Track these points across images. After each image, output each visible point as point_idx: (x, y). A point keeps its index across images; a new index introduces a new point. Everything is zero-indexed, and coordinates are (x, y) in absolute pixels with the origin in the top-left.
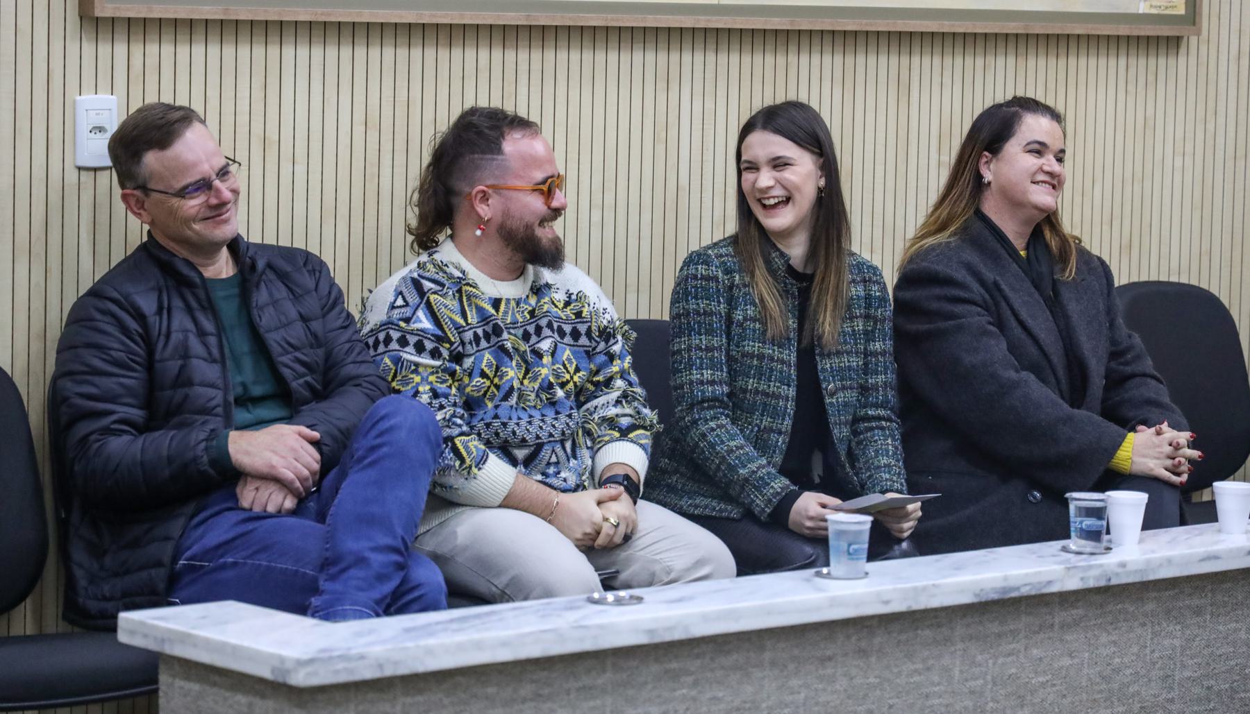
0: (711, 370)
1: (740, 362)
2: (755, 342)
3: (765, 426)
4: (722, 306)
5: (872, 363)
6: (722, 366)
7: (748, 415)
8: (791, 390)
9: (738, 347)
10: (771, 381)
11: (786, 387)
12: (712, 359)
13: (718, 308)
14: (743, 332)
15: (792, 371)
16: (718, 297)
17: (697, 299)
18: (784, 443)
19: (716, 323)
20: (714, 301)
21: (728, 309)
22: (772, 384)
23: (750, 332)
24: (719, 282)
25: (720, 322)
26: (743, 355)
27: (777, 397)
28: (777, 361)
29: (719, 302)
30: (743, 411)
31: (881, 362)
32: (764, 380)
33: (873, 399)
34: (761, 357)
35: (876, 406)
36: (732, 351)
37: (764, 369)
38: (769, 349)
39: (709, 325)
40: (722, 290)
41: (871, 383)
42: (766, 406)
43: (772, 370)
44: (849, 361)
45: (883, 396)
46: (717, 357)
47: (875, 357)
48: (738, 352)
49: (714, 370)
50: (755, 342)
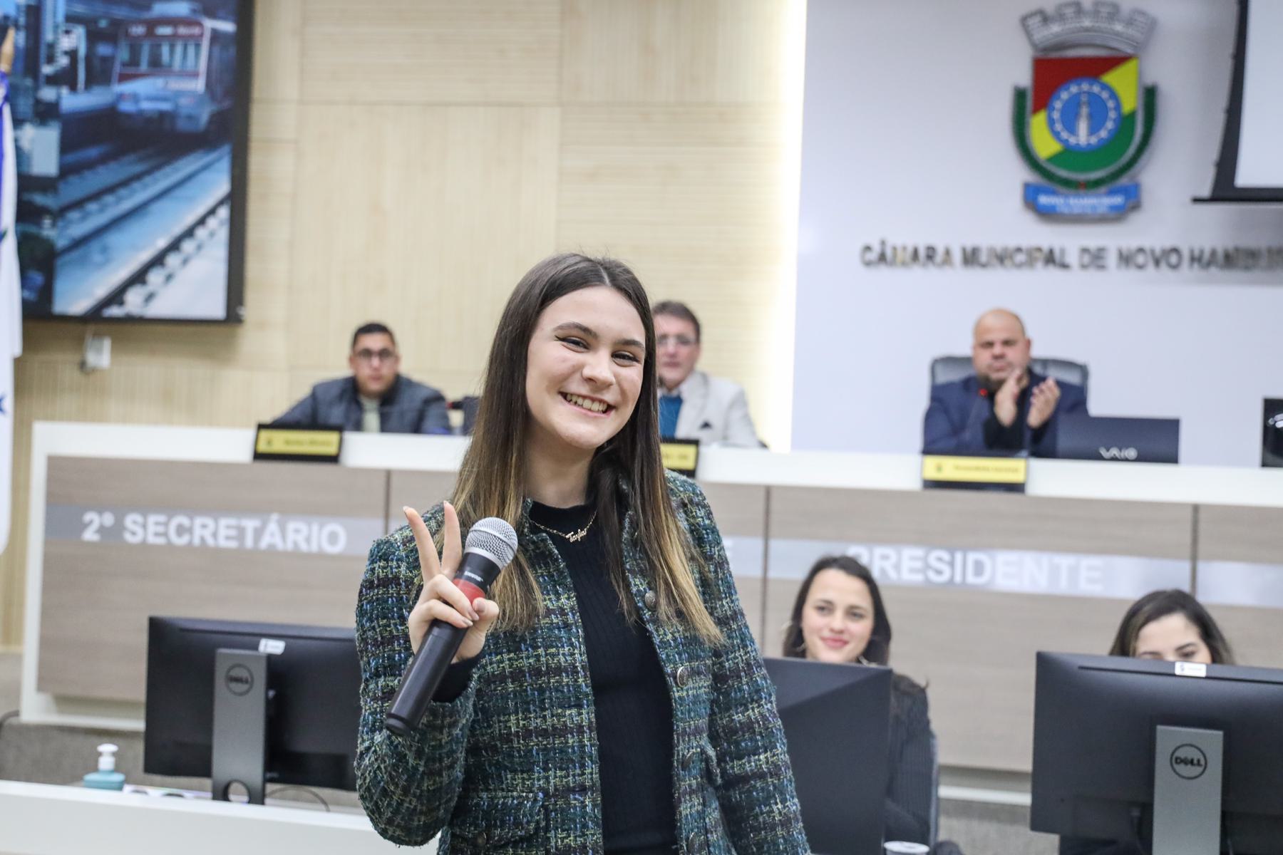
2: (501, 653)
3: (555, 786)
7: (525, 775)
8: (584, 711)
10: (544, 709)
11: (574, 711)
15: (580, 680)
18: (594, 806)
22: (547, 713)
27: (562, 731)
30: (514, 771)
32: (535, 711)
34: (517, 675)
37: (529, 692)
38: (528, 658)
42: (548, 754)
43: (541, 691)
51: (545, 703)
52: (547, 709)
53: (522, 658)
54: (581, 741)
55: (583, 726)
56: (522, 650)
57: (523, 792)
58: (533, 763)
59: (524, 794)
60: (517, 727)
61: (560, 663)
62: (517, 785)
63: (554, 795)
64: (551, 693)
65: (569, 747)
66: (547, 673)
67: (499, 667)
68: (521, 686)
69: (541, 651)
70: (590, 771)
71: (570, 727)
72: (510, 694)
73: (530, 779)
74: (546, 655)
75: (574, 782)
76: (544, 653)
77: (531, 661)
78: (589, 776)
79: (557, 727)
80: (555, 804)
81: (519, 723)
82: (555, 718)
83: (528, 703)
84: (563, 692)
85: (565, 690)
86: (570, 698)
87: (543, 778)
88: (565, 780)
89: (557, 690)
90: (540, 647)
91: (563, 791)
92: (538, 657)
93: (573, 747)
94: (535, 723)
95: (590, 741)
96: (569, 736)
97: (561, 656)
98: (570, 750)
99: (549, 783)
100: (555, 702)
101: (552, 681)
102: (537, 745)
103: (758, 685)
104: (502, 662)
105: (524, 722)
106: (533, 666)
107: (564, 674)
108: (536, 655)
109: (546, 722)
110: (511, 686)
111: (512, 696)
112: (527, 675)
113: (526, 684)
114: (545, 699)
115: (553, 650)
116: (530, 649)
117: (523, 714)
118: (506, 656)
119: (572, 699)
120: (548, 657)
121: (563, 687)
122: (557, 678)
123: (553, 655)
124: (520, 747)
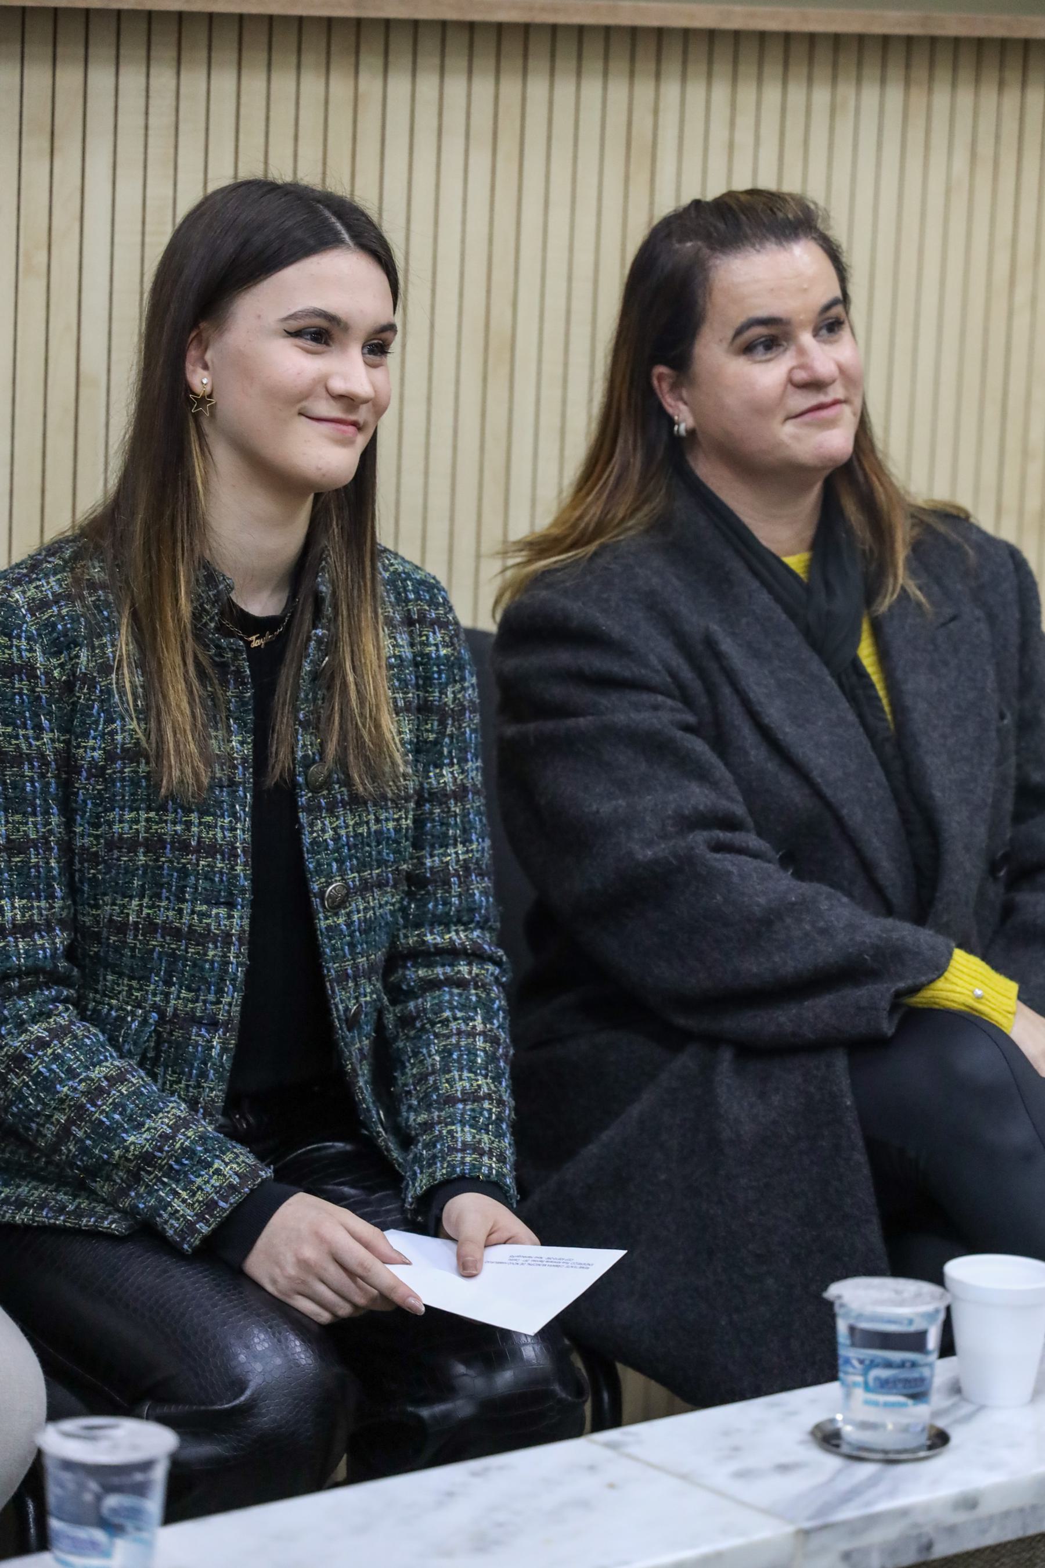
1: (105, 862)
2: (138, 809)
3: (176, 1009)
4: (46, 737)
7: (134, 983)
8: (236, 914)
10: (184, 901)
11: (223, 911)
15: (239, 868)
16: (36, 715)
19: (32, 781)
20: (24, 726)
21: (64, 741)
22: (187, 907)
24: (37, 677)
26: (110, 845)
27: (203, 938)
28: (197, 851)
30: (121, 975)
32: (168, 898)
34: (155, 845)
36: (82, 836)
38: (174, 823)
39: (14, 788)
40: (43, 696)
42: (174, 963)
43: (184, 873)
44: (378, 821)
48: (97, 837)
51: (185, 892)
52: (187, 901)
53: (166, 822)
54: (225, 956)
55: (233, 935)
56: (167, 811)
57: (127, 1003)
58: (151, 970)
59: (129, 1008)
60: (138, 917)
61: (216, 840)
62: (120, 992)
63: (170, 1022)
64: (197, 880)
65: (206, 961)
67: (131, 828)
68: (157, 860)
69: (194, 817)
70: (228, 1000)
71: (214, 933)
72: (137, 869)
73: (140, 989)
74: (200, 824)
75: (203, 1011)
77: (178, 828)
78: (227, 1008)
79: (196, 930)
80: (171, 1034)
81: (142, 911)
82: (195, 917)
83: (162, 886)
84: (212, 881)
85: (217, 879)
86: (220, 891)
87: (161, 994)
88: (190, 1005)
89: (206, 878)
90: (193, 812)
91: (184, 1019)
92: (188, 824)
93: (212, 962)
94: (165, 914)
95: (237, 957)
96: (210, 945)
97: (218, 830)
98: (207, 966)
99: (168, 1002)
100: (201, 894)
101: (202, 863)
102: (162, 946)
103: (474, 901)
104: (137, 821)
105: (149, 911)
106: (180, 836)
107: (219, 857)
108: (186, 821)
109: (181, 918)
110: (142, 858)
111: (140, 872)
112: (169, 846)
113: (163, 859)
114: (186, 886)
115: (209, 819)
116: (179, 810)
117: (150, 899)
118: (143, 815)
119: (223, 894)
121: (215, 873)
122: (210, 859)
123: (209, 827)
124: (135, 944)
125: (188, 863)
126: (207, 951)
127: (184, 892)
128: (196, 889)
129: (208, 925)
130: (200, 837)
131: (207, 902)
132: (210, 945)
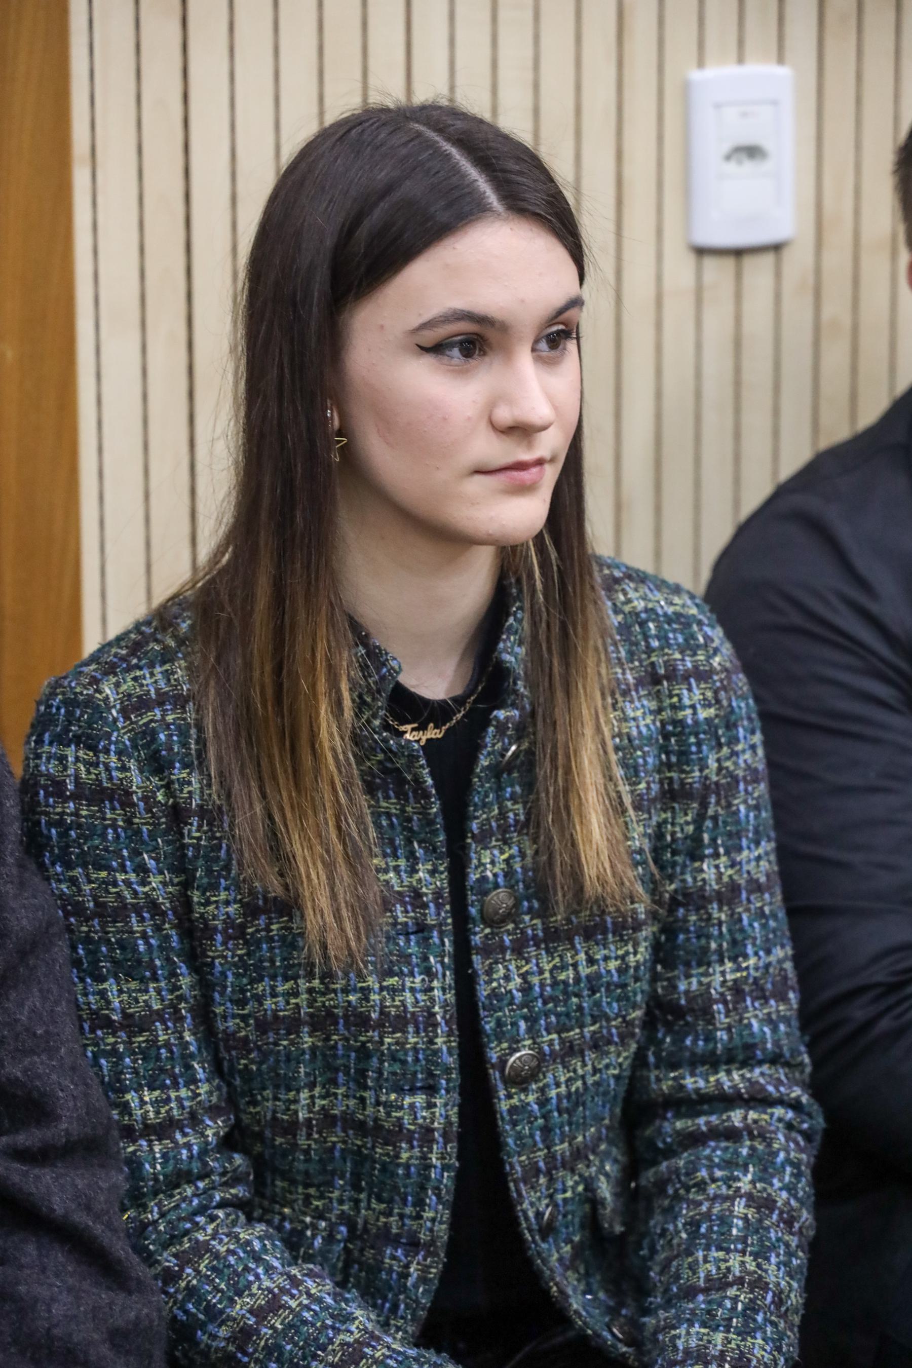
0: (152, 1089)
1: (259, 1048)
5: (687, 931)
6: (188, 1067)
8: (439, 1101)
9: (242, 1003)
10: (366, 1088)
11: (419, 1099)
12: (149, 1053)
13: (140, 889)
14: (248, 954)
15: (439, 1040)
17: (69, 866)
19: (144, 936)
23: (271, 949)
25: (158, 929)
26: (263, 1027)
28: (380, 1025)
29: (141, 869)
31: (720, 924)
33: (695, 1042)
35: (713, 1062)
36: (225, 1017)
38: (346, 991)
39: (123, 948)
41: (687, 992)
43: (364, 1053)
45: (729, 1029)
46: (167, 1045)
47: (698, 910)
48: (244, 1018)
49: (163, 1087)
50: (295, 978)
54: (424, 1157)
64: (381, 1062)
65: (398, 1165)
66: (380, 1025)
67: (288, 1003)
68: (328, 1039)
71: (408, 1130)
74: (382, 989)
76: (377, 986)
78: (429, 1224)
79: (383, 1126)
82: (381, 1109)
84: (404, 1062)
85: (410, 1059)
86: (415, 1073)
89: (394, 1058)
93: (407, 1166)
96: (404, 1145)
97: (408, 994)
98: (400, 1172)
100: (387, 1080)
101: (387, 1040)
106: (355, 1008)
108: (362, 988)
110: (307, 1039)
111: (307, 1057)
112: (341, 1021)
115: (393, 981)
119: (420, 1076)
120: (385, 993)
121: (406, 1054)
122: (399, 1035)
123: (394, 991)
125: (368, 1042)
126: (399, 1153)
127: (365, 1077)
128: (380, 1072)
129: (400, 1119)
130: (383, 1007)
131: (400, 1090)
132: (404, 1145)
